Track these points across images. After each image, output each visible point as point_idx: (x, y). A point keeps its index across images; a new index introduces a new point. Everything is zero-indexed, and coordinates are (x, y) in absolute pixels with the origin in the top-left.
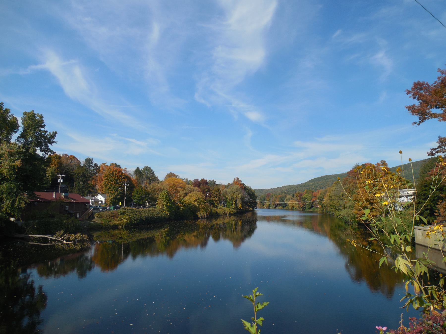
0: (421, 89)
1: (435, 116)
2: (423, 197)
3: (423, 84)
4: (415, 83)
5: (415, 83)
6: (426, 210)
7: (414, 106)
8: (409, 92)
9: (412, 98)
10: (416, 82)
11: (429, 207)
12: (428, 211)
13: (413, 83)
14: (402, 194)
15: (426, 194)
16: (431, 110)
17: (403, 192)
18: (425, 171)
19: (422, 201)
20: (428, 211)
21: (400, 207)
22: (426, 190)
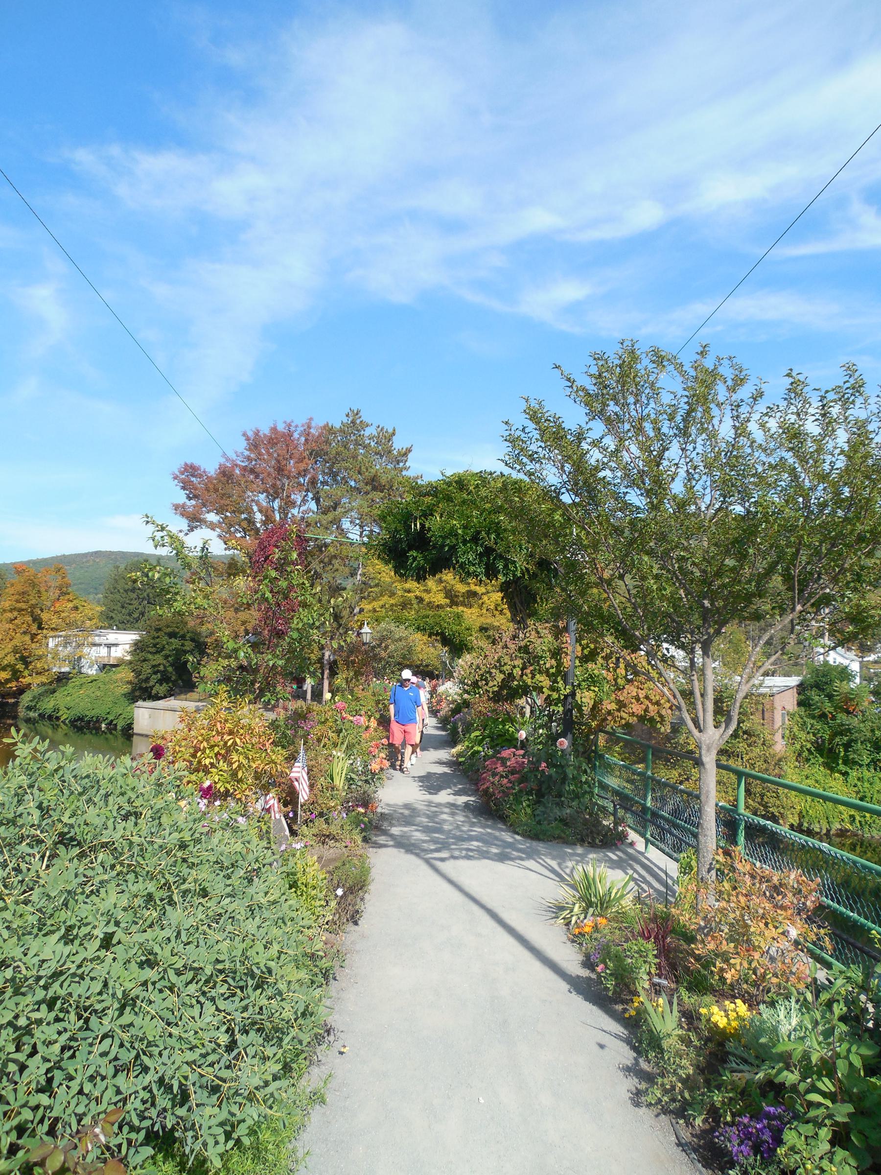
0: (193, 476)
1: (212, 526)
2: (153, 650)
3: (199, 469)
4: (186, 464)
5: (186, 464)
6: (155, 673)
7: (183, 506)
8: (175, 478)
9: (178, 488)
10: (189, 462)
11: (161, 668)
12: (159, 675)
13: (183, 464)
14: (97, 640)
15: (157, 644)
16: (207, 515)
17: (99, 636)
18: (115, 588)
19: (150, 656)
20: (159, 675)
21: (90, 667)
22: (158, 637)
